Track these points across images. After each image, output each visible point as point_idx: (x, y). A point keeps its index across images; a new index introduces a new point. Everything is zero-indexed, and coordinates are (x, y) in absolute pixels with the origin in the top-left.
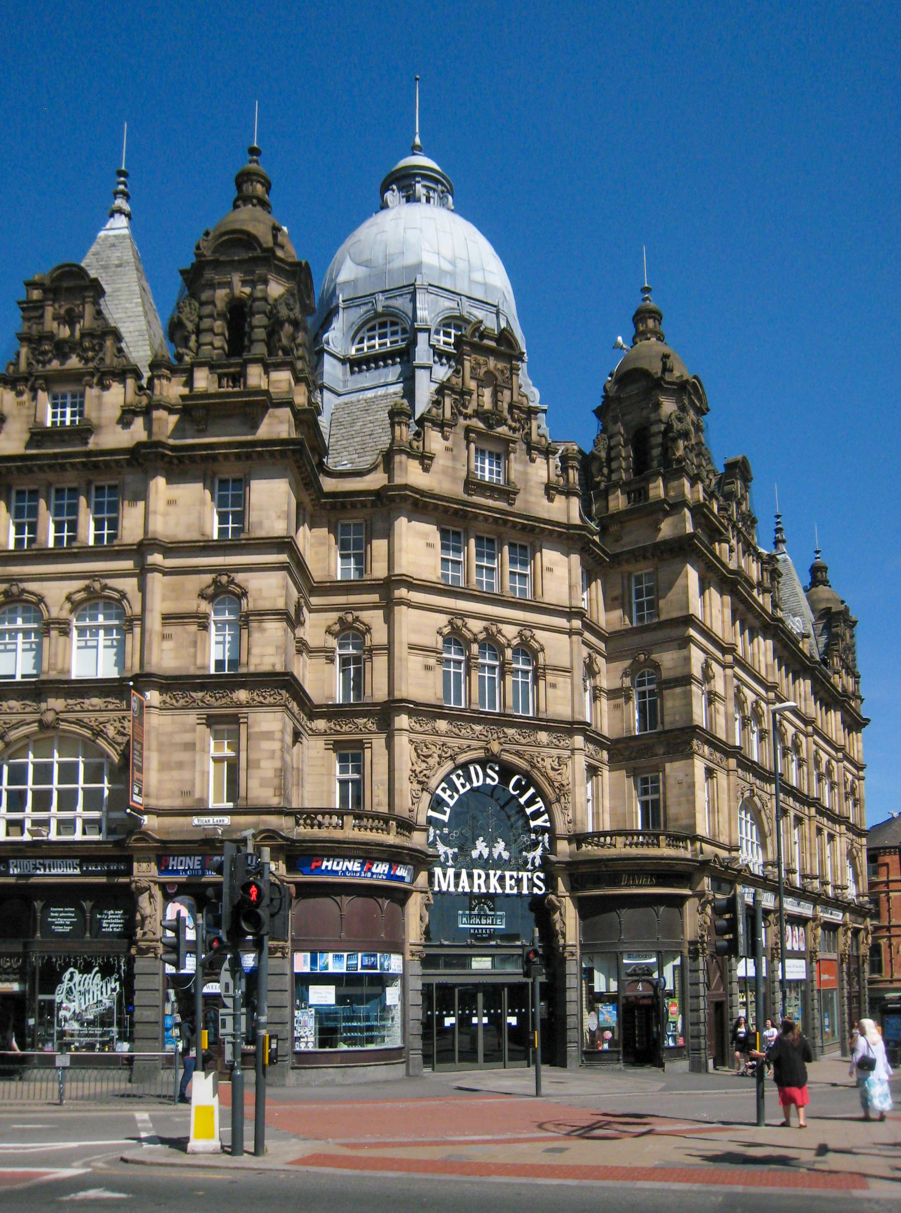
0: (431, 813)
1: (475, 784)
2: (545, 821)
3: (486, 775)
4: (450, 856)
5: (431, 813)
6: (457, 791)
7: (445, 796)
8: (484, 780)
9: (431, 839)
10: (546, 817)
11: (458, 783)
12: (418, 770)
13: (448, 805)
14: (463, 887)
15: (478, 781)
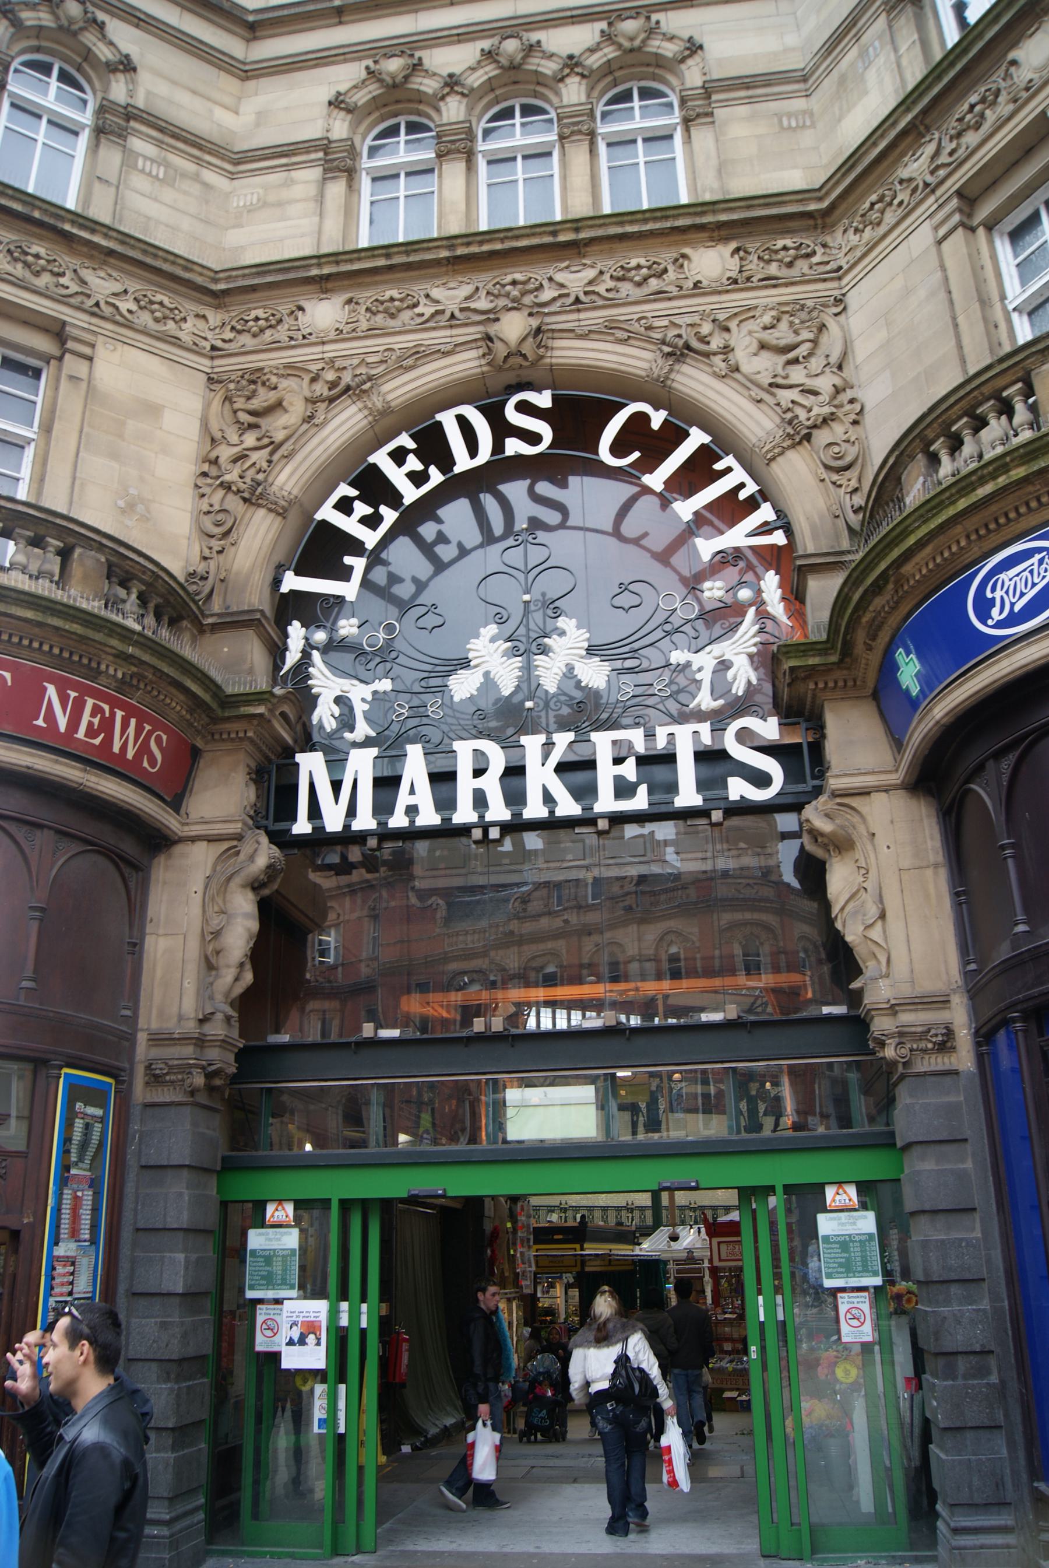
0: (292, 582)
1: (463, 463)
2: (765, 529)
3: (502, 430)
4: (360, 708)
5: (292, 582)
6: (394, 498)
7: (350, 525)
8: (498, 447)
9: (292, 657)
10: (766, 513)
11: (397, 476)
12: (225, 453)
13: (356, 547)
14: (412, 810)
15: (473, 451)
